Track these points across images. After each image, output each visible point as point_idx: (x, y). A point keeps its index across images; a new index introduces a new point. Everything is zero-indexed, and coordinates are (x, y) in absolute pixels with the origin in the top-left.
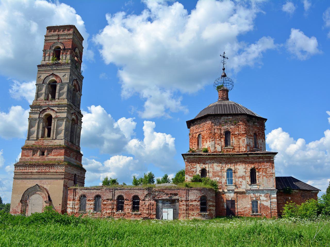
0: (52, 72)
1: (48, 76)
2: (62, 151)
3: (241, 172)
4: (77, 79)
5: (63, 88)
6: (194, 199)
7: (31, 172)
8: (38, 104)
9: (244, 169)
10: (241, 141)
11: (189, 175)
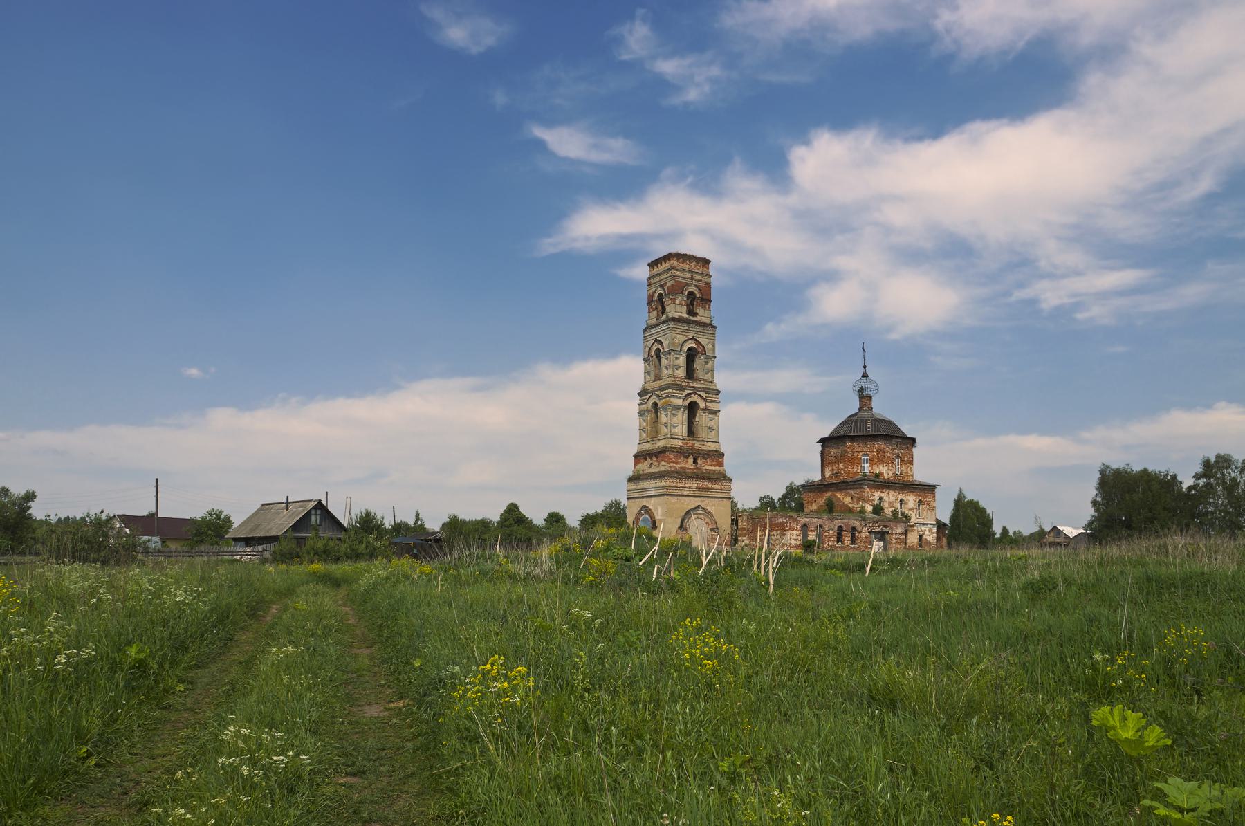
0: (691, 334)
1: (686, 340)
5: (707, 363)
8: (678, 383)
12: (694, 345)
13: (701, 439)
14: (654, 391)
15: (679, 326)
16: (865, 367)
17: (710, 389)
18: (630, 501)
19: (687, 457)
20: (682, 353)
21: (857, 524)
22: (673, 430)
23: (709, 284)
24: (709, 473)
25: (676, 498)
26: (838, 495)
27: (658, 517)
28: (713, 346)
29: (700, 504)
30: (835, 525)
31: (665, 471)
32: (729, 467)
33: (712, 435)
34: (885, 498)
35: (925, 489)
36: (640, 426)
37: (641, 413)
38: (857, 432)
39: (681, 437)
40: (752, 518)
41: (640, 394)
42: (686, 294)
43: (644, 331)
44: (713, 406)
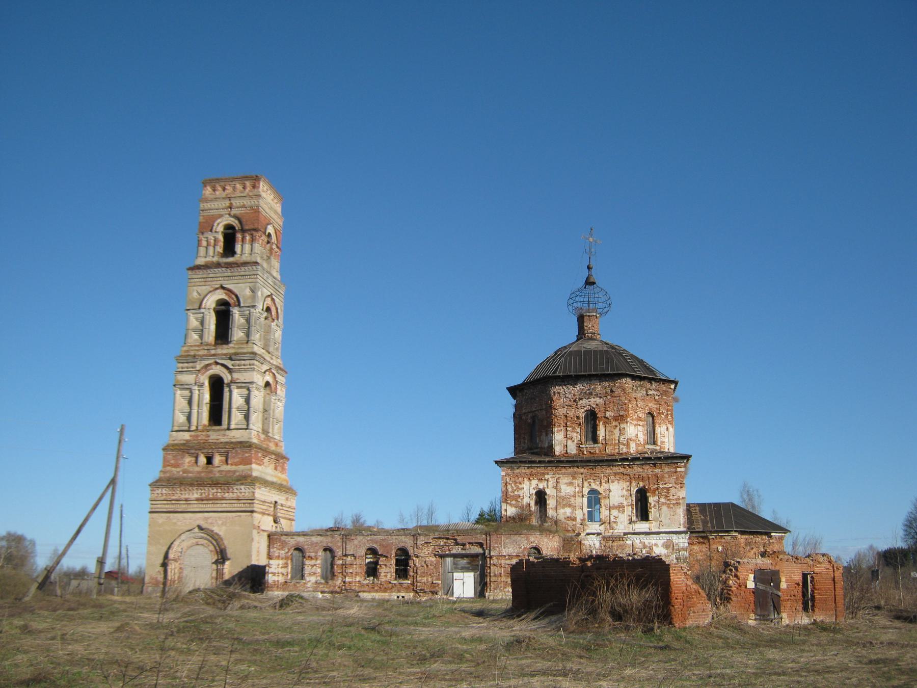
2: (247, 455)
3: (617, 496)
4: (272, 294)
6: (515, 554)
7: (186, 500)
8: (192, 353)
9: (622, 490)
11: (511, 505)
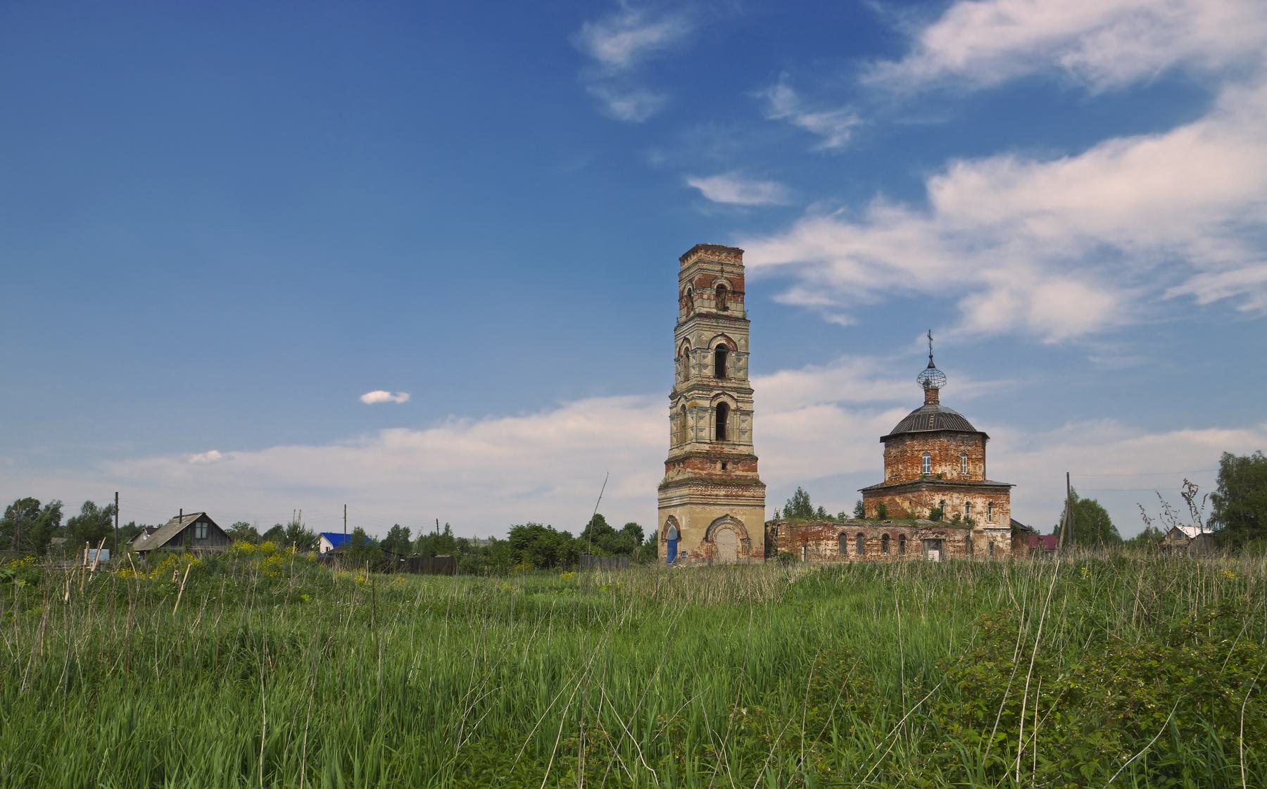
0: (721, 330)
1: (715, 337)
5: (739, 360)
7: (716, 495)
8: (705, 383)
10: (977, 468)
12: (724, 342)
13: (732, 442)
14: (683, 393)
15: (707, 322)
16: (931, 357)
17: (741, 388)
18: (661, 510)
19: (715, 462)
20: (710, 350)
21: (906, 531)
22: (700, 434)
23: (743, 275)
24: (740, 479)
25: (701, 506)
26: (898, 499)
27: (683, 527)
28: (746, 341)
29: (728, 513)
30: (879, 533)
31: (689, 479)
32: (762, 475)
33: (745, 438)
34: (947, 502)
35: (997, 490)
36: (671, 430)
37: (672, 418)
38: (917, 429)
39: (708, 441)
40: (791, 527)
41: (671, 397)
42: (715, 287)
43: (675, 330)
44: (745, 407)
